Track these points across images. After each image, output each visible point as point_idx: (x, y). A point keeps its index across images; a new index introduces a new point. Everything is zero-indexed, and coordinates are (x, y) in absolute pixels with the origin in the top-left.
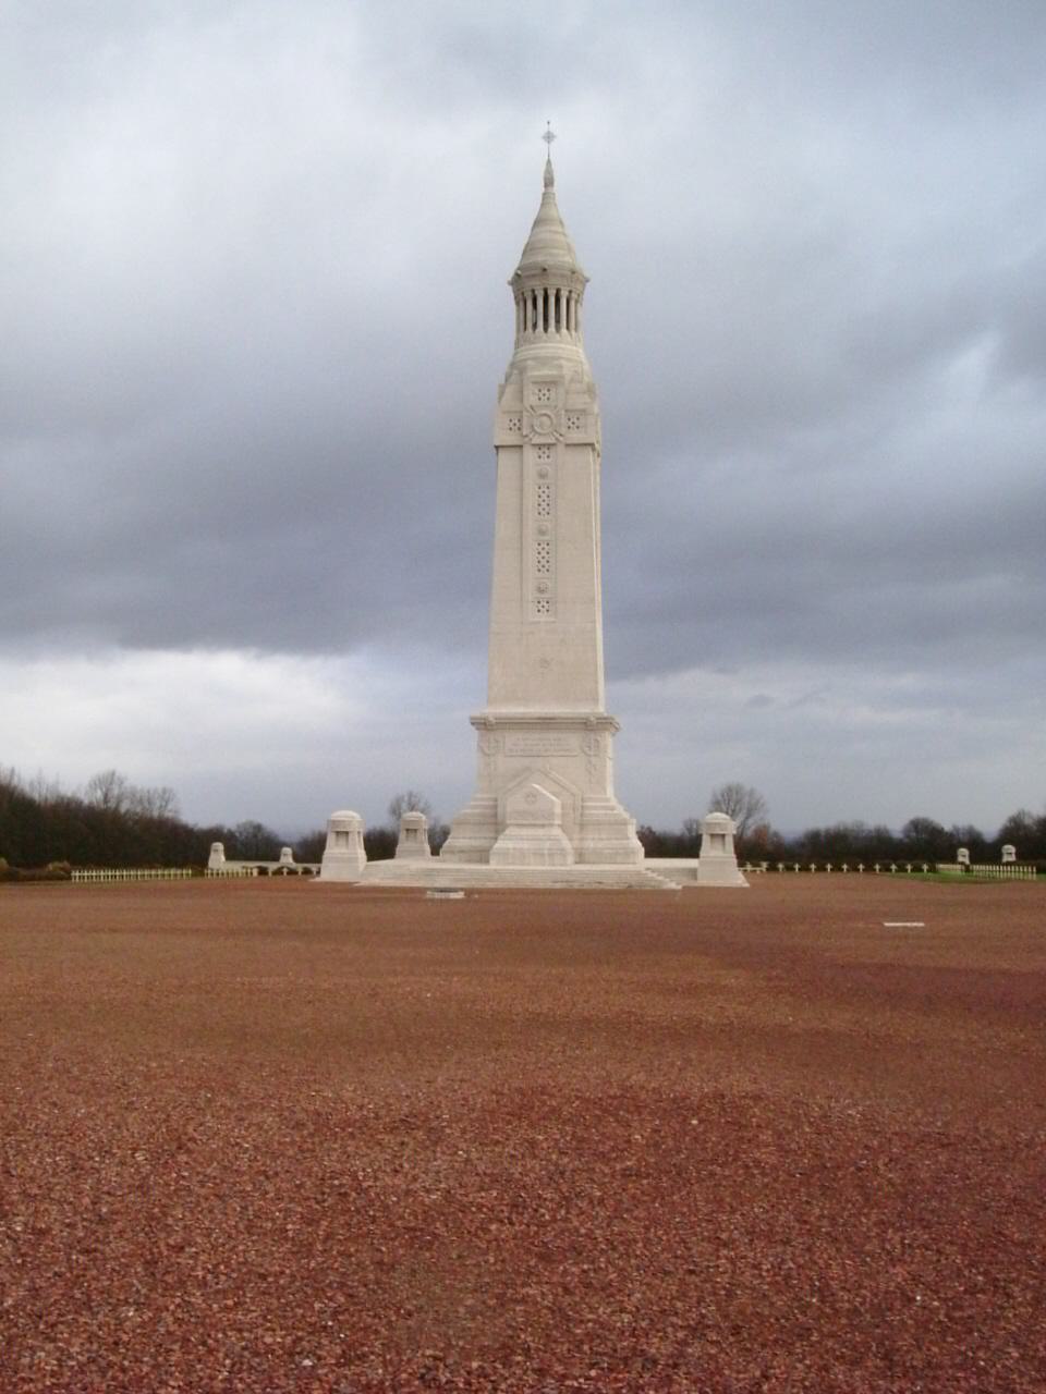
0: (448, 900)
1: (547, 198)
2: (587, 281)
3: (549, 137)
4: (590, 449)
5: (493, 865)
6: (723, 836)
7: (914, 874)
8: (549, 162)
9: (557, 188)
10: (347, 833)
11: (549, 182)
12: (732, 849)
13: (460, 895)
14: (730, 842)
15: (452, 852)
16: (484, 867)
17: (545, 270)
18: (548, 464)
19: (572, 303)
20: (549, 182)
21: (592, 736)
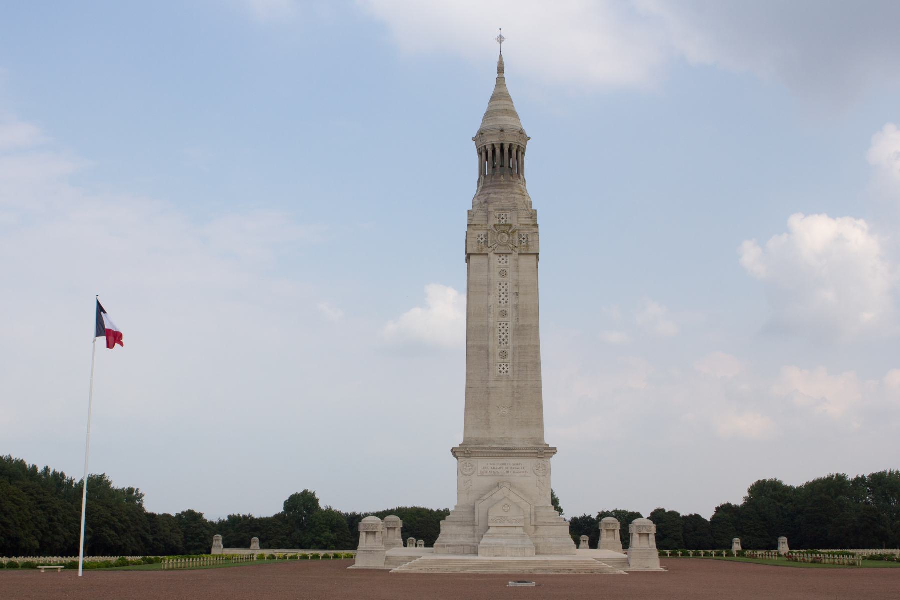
0: (528, 588)
1: (501, 82)
2: (529, 139)
3: (501, 39)
4: (534, 257)
5: (479, 558)
6: (648, 535)
7: (728, 558)
8: (501, 56)
9: (505, 75)
10: (375, 533)
11: (501, 70)
12: (655, 544)
13: (533, 584)
14: (652, 538)
15: (444, 546)
16: (477, 558)
17: (502, 131)
18: (507, 267)
19: (520, 154)
20: (501, 70)
21: (541, 461)
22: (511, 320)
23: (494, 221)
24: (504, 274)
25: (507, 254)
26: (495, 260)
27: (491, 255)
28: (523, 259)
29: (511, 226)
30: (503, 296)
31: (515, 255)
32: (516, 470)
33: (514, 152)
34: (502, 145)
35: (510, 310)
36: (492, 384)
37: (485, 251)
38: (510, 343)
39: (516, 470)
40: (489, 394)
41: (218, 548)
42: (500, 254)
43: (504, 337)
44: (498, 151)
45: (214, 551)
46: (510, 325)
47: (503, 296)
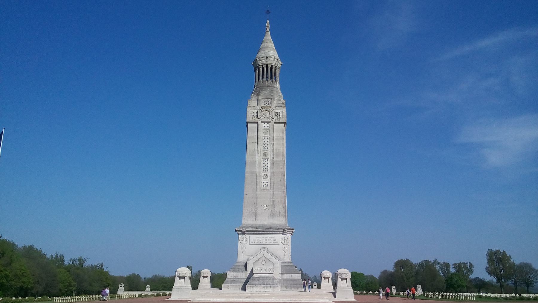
14: (349, 280)
22: (269, 157)
23: (262, 104)
24: (266, 133)
25: (268, 122)
26: (262, 125)
27: (260, 122)
28: (276, 125)
29: (270, 107)
30: (266, 145)
31: (273, 123)
32: (271, 241)
33: (274, 70)
34: (267, 65)
35: (269, 152)
36: (258, 193)
37: (257, 120)
38: (269, 171)
39: (271, 241)
40: (257, 198)
41: (122, 291)
42: (264, 122)
43: (266, 167)
44: (265, 69)
45: (119, 293)
46: (269, 162)
47: (266, 145)
